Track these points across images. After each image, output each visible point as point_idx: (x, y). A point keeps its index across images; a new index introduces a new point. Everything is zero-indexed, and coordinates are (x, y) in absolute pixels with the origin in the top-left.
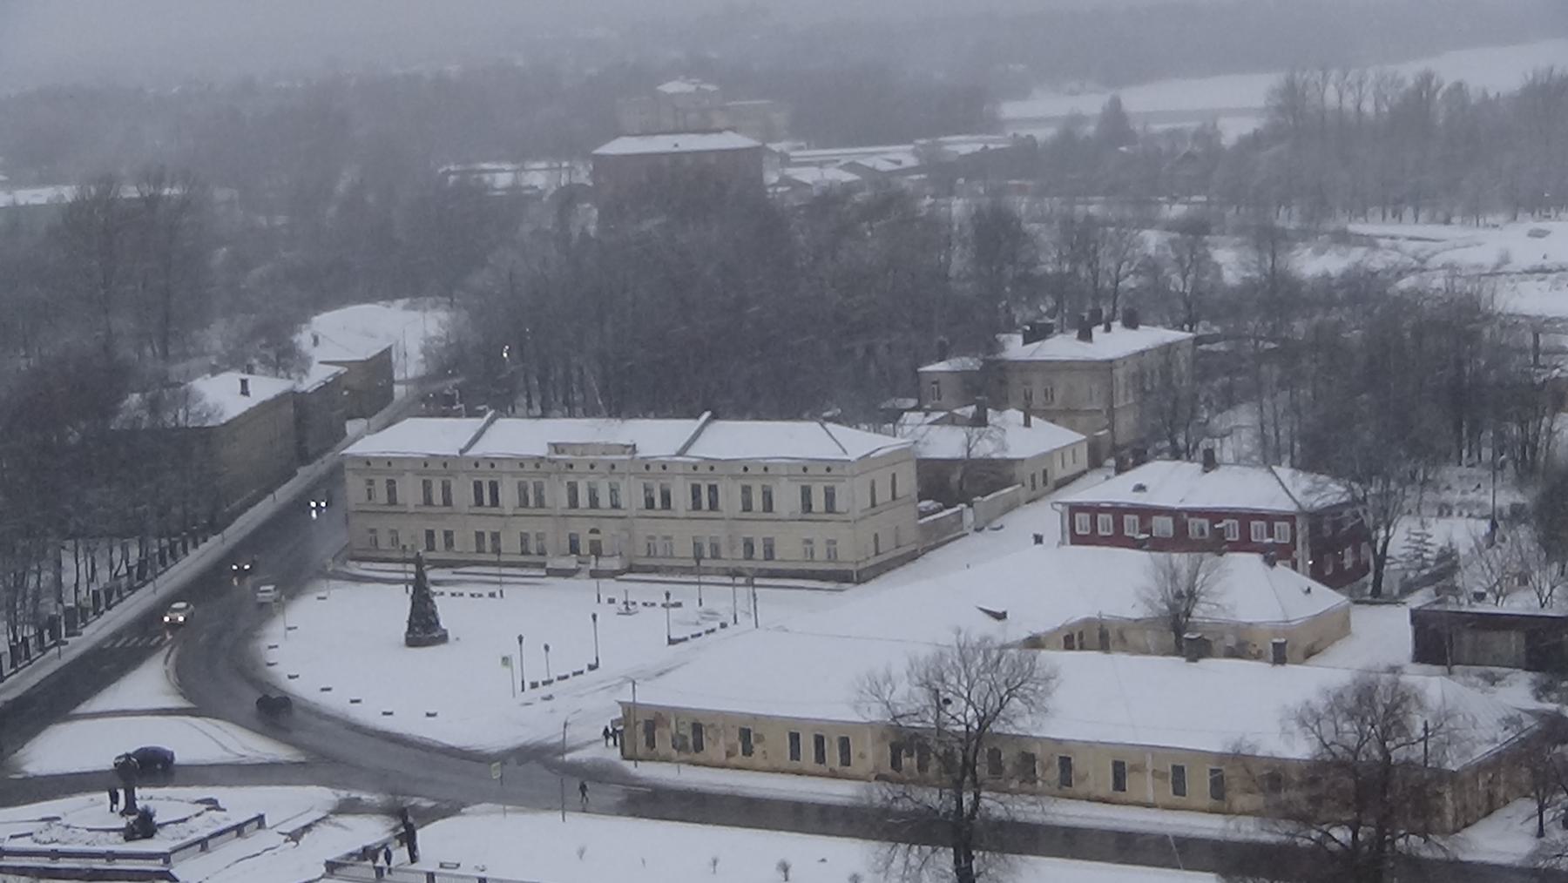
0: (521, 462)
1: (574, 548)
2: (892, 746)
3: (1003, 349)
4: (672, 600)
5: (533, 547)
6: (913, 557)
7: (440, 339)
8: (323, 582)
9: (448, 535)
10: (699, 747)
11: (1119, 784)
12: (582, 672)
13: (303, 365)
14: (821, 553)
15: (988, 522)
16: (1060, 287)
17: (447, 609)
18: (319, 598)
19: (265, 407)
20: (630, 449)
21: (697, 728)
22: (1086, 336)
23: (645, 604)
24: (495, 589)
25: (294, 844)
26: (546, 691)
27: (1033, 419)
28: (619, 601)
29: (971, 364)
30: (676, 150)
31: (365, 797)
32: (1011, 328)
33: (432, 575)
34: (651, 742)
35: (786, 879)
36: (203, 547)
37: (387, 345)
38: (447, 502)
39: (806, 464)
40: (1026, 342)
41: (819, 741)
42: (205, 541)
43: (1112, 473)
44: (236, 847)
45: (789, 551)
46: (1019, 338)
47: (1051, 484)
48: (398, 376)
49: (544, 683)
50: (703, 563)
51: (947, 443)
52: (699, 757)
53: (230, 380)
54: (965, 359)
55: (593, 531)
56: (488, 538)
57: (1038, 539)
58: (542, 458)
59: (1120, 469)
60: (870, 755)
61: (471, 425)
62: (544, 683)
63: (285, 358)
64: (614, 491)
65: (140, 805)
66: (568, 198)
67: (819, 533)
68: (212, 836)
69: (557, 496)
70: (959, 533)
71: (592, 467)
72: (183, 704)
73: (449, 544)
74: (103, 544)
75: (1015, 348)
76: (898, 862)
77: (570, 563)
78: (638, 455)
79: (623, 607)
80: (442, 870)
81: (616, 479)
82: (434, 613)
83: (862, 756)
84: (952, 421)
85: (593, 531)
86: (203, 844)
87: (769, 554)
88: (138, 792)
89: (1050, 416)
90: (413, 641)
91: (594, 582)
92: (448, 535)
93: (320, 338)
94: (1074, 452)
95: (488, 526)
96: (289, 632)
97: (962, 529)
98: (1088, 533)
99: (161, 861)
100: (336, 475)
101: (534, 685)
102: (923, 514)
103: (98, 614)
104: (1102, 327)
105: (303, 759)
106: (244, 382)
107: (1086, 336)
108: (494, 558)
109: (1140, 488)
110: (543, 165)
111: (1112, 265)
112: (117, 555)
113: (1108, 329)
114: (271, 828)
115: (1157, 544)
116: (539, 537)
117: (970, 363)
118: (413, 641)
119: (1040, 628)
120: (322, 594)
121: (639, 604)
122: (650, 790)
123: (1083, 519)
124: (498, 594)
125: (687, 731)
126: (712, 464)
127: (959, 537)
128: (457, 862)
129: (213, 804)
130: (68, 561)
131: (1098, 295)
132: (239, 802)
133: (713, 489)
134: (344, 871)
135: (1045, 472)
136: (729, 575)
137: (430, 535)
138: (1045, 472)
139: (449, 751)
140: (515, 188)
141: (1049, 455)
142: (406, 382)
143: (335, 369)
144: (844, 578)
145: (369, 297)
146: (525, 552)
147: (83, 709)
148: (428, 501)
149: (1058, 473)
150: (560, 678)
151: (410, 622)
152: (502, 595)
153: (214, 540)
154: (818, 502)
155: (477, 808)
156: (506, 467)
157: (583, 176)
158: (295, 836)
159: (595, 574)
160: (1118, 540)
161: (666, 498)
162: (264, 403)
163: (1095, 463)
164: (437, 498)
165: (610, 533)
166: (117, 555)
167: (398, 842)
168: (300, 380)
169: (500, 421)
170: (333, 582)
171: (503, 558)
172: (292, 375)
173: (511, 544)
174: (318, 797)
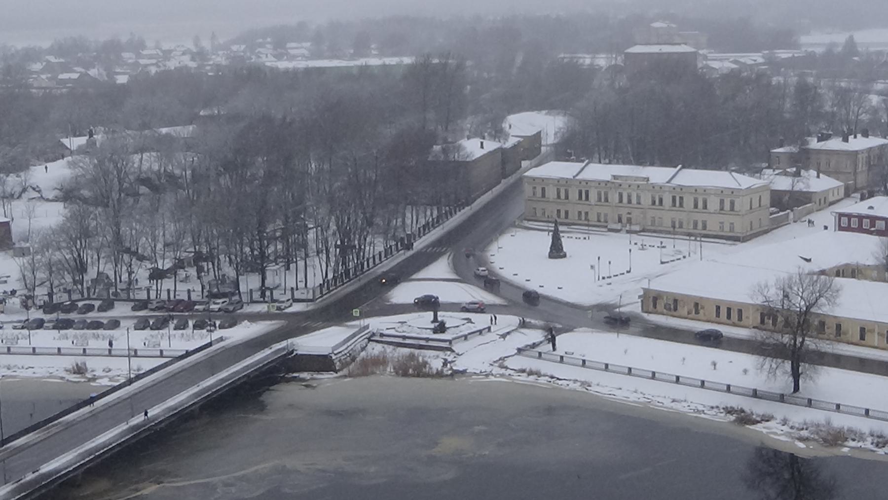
1: (620, 220)
2: (762, 314)
3: (808, 144)
4: (663, 245)
6: (766, 232)
7: (564, 128)
8: (514, 229)
9: (567, 213)
10: (676, 309)
11: (862, 338)
12: (623, 274)
13: (506, 136)
14: (727, 228)
15: (799, 219)
16: (831, 118)
17: (567, 244)
18: (512, 236)
19: (491, 153)
20: (646, 180)
21: (676, 301)
22: (846, 140)
23: (650, 246)
24: (586, 236)
25: (503, 339)
26: (609, 281)
27: (821, 175)
28: (639, 244)
29: (794, 150)
30: (660, 51)
31: (533, 321)
32: (810, 134)
33: (561, 228)
34: (655, 306)
35: (715, 369)
36: (463, 211)
37: (539, 130)
38: (567, 197)
39: (723, 189)
40: (818, 141)
41: (729, 310)
42: (463, 208)
43: (859, 200)
44: (479, 339)
45: (713, 226)
46: (816, 140)
47: (827, 204)
48: (543, 143)
49: (608, 277)
50: (676, 229)
51: (783, 183)
52: (675, 313)
53: (476, 141)
54: (792, 147)
55: (629, 213)
56: (583, 214)
57: (826, 228)
58: (608, 181)
59: (863, 198)
60: (753, 318)
61: (578, 166)
62: (608, 277)
63: (498, 133)
64: (638, 197)
65: (439, 319)
66: (615, 70)
67: (727, 219)
68: (470, 334)
69: (614, 197)
70: (787, 223)
71: (629, 186)
72: (454, 277)
73: (567, 217)
74: (422, 208)
75: (814, 144)
76: (767, 366)
77: (618, 226)
78: (649, 182)
79: (641, 247)
80: (566, 355)
81: (639, 192)
82: (561, 245)
83: (747, 318)
84: (786, 174)
85: (629, 213)
86: (466, 337)
87: (704, 227)
88: (439, 313)
89: (828, 174)
90: (551, 256)
91: (628, 235)
92: (567, 213)
93: (512, 126)
94: (838, 189)
95: (583, 209)
96: (500, 249)
97: (788, 221)
98: (846, 226)
99: (448, 343)
100: (517, 185)
101: (604, 278)
102: (771, 214)
103: (420, 237)
104: (853, 136)
105: (506, 304)
106: (482, 143)
107: (846, 140)
108: (586, 222)
109: (871, 208)
110: (604, 56)
111: (856, 109)
112: (429, 213)
113: (855, 137)
114: (494, 332)
115: (879, 233)
116: (606, 215)
117: (793, 149)
118: (551, 256)
119: (825, 267)
120: (513, 234)
121: (648, 245)
122: (653, 326)
123: (845, 220)
124: (587, 238)
125: (671, 302)
126: (681, 187)
127: (786, 225)
128: (572, 351)
129: (469, 321)
130: (409, 215)
131: (848, 122)
132: (481, 320)
133: (681, 198)
134: (524, 353)
135: (825, 198)
136: (688, 235)
137: (559, 211)
138: (825, 198)
139: (567, 304)
140: (591, 65)
141: (827, 191)
142: (547, 145)
143: (518, 139)
144: (736, 239)
145: (531, 109)
146: (599, 221)
147: (414, 277)
148: (559, 197)
149: (831, 199)
150: (614, 276)
151: (551, 248)
152: (589, 238)
153: (467, 208)
154: (727, 206)
155: (581, 329)
156: (593, 184)
157: (620, 60)
158: (503, 336)
159: (628, 232)
160: (860, 229)
161: (661, 201)
162: (490, 152)
163: (847, 195)
164: (563, 196)
165: (636, 214)
166: (429, 213)
167: (547, 341)
168: (505, 143)
169: (591, 165)
170: (518, 229)
171: (591, 223)
172: (501, 141)
173: (593, 217)
174: (515, 320)
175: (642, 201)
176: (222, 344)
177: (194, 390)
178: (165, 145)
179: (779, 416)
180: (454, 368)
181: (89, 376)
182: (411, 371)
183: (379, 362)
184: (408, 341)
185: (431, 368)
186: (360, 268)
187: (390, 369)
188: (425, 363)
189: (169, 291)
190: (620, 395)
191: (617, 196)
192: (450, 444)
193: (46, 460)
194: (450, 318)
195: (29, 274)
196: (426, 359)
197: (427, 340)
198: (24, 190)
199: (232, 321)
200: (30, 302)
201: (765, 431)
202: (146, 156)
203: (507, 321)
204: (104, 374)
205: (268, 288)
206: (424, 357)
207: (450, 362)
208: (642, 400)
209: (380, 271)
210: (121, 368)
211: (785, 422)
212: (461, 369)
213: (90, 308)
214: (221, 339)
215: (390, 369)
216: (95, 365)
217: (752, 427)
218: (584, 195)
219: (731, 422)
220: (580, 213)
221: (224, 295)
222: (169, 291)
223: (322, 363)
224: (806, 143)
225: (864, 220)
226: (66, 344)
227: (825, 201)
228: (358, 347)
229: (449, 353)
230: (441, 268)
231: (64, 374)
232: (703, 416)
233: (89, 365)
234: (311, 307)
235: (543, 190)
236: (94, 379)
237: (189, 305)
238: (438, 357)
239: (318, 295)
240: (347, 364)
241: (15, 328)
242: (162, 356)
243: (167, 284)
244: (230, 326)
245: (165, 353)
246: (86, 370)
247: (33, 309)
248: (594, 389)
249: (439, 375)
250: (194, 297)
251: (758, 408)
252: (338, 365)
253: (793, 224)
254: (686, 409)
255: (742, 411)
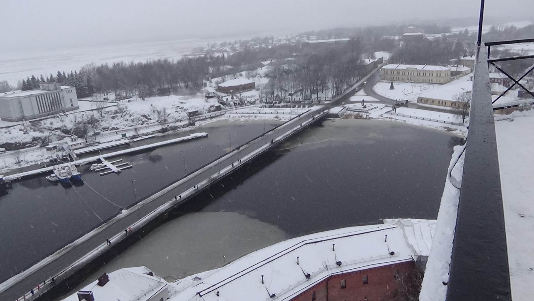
0: (403, 70)
1: (408, 79)
5: (403, 79)
9: (393, 78)
14: (438, 80)
17: (395, 86)
22: (471, 57)
38: (393, 73)
45: (434, 81)
46: (462, 57)
51: (454, 69)
64: (413, 73)
67: (438, 79)
75: (462, 58)
77: (408, 81)
84: (454, 66)
85: (411, 78)
90: (390, 89)
91: (411, 83)
92: (393, 78)
107: (471, 57)
112: (357, 78)
116: (404, 78)
118: (390, 89)
126: (426, 70)
133: (426, 73)
141: (466, 71)
149: (467, 73)
154: (439, 75)
159: (410, 82)
161: (420, 74)
166: (357, 78)
173: (400, 78)
175: (414, 74)
176: (310, 111)
177: (307, 122)
178: (289, 63)
179: (459, 129)
180: (370, 117)
181: (279, 119)
182: (358, 118)
183: (350, 115)
184: (357, 110)
185: (363, 117)
186: (341, 93)
187: (353, 117)
188: (362, 116)
189: (295, 99)
190: (414, 124)
191: (407, 73)
192: (372, 135)
193: (278, 137)
194: (367, 105)
195: (261, 94)
196: (362, 115)
197: (362, 110)
198: (256, 75)
199: (311, 105)
200: (262, 101)
201: (455, 133)
202: (285, 65)
203: (383, 105)
204: (283, 118)
205: (319, 98)
206: (361, 114)
207: (368, 115)
208: (421, 125)
209: (346, 93)
210: (287, 117)
211: (461, 131)
212: (371, 117)
213: (276, 103)
214: (310, 110)
215: (353, 117)
216: (280, 116)
217: (452, 132)
218: (398, 73)
219: (446, 130)
220: (397, 78)
221: (309, 99)
222: (295, 99)
223: (336, 116)
224: (460, 58)
226: (273, 111)
227: (466, 74)
228: (344, 112)
229: (367, 113)
230: (362, 92)
231: (273, 118)
232: (438, 129)
233: (279, 116)
234: (330, 102)
235: (387, 72)
236: (280, 119)
237: (300, 102)
238: (364, 114)
239: (332, 99)
240: (342, 116)
241: (259, 108)
242: (296, 114)
243: (294, 97)
244: (312, 107)
245: (297, 113)
246: (278, 117)
247: (262, 103)
248: (407, 122)
249: (366, 118)
250: (301, 100)
251: (453, 127)
252: (340, 116)
253: (457, 80)
254: (433, 127)
255: (448, 128)
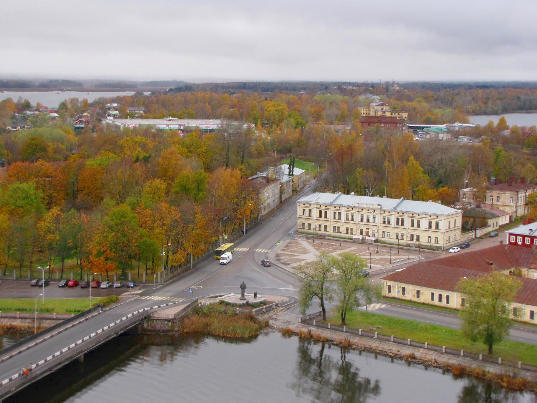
55: (367, 229)
81: (374, 214)
85: (367, 229)
92: (325, 226)
95: (337, 225)
135: (497, 223)
137: (320, 226)
138: (497, 223)
154: (434, 226)
225: (526, 238)
